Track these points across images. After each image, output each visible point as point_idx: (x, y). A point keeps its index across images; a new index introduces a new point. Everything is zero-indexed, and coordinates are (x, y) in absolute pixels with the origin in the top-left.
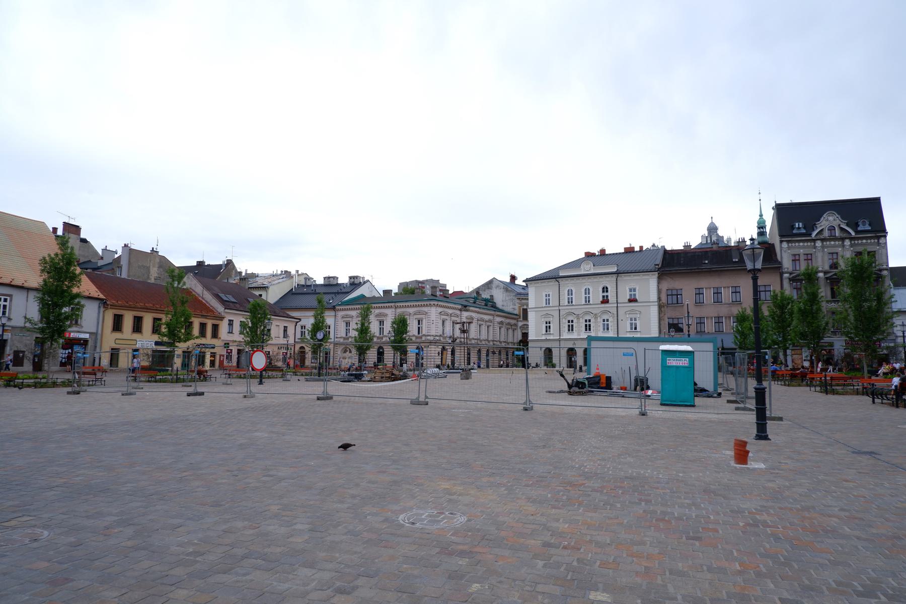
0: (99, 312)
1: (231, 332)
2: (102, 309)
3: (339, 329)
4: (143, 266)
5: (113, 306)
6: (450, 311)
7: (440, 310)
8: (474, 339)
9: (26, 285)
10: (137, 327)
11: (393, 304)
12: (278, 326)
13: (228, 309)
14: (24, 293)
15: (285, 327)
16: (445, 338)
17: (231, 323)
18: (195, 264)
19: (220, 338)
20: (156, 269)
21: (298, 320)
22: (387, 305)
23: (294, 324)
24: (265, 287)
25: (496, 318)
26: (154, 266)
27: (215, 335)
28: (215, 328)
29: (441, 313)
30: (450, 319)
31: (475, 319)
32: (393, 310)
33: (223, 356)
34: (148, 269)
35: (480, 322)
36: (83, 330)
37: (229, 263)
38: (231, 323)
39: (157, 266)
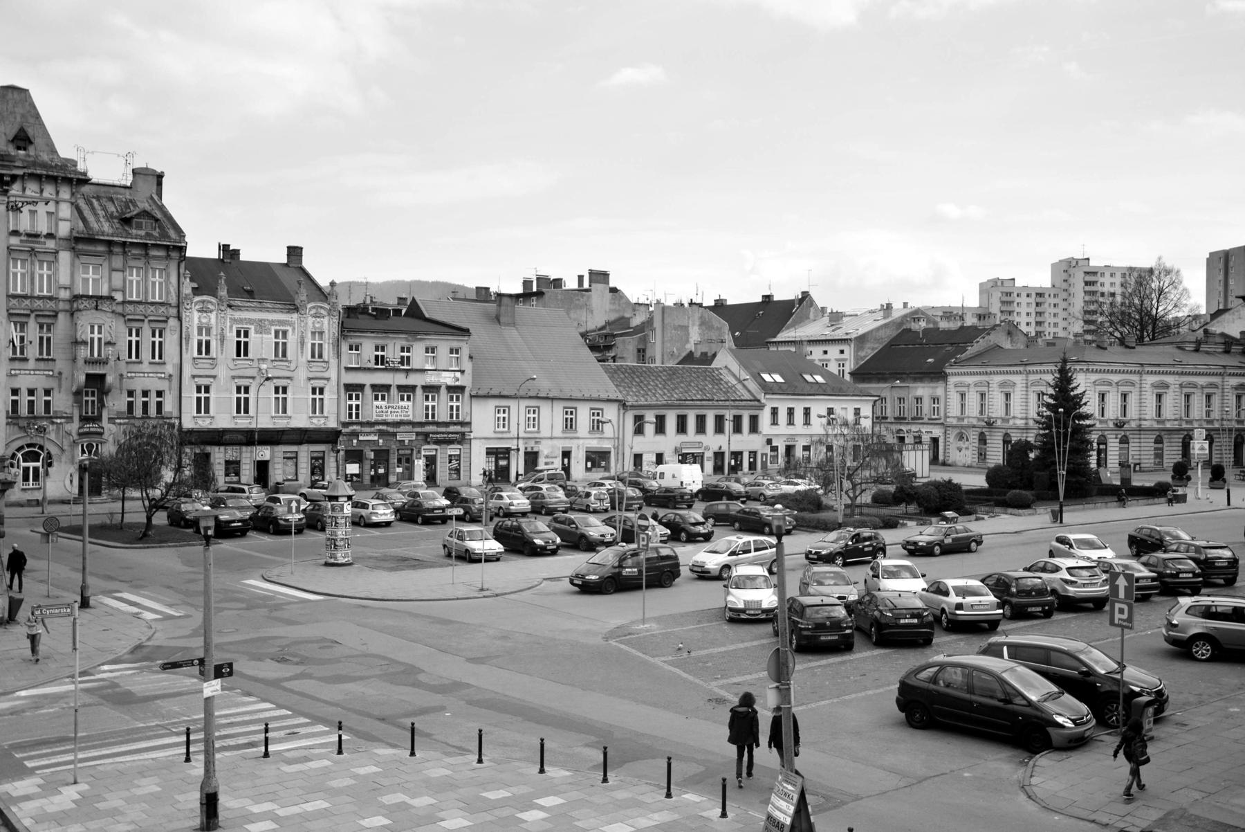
0: (619, 415)
1: (775, 422)
2: (622, 411)
3: (951, 404)
4: (679, 326)
5: (633, 407)
6: (1115, 378)
7: (1094, 377)
8: (1168, 420)
9: (551, 395)
10: (660, 428)
11: (1021, 368)
12: (846, 408)
13: (769, 393)
14: (549, 402)
15: (855, 409)
16: (1106, 422)
17: (775, 412)
18: (760, 300)
19: (761, 433)
20: (696, 328)
21: (877, 398)
22: (1015, 369)
23: (871, 404)
24: (847, 340)
25: (1227, 379)
26: (693, 325)
27: (754, 428)
28: (754, 420)
29: (1094, 382)
30: (1116, 389)
31: (1172, 387)
32: (1023, 376)
33: (766, 455)
34: (685, 328)
35: (1185, 390)
36: (605, 435)
37: (805, 295)
38: (775, 412)
39: (697, 323)
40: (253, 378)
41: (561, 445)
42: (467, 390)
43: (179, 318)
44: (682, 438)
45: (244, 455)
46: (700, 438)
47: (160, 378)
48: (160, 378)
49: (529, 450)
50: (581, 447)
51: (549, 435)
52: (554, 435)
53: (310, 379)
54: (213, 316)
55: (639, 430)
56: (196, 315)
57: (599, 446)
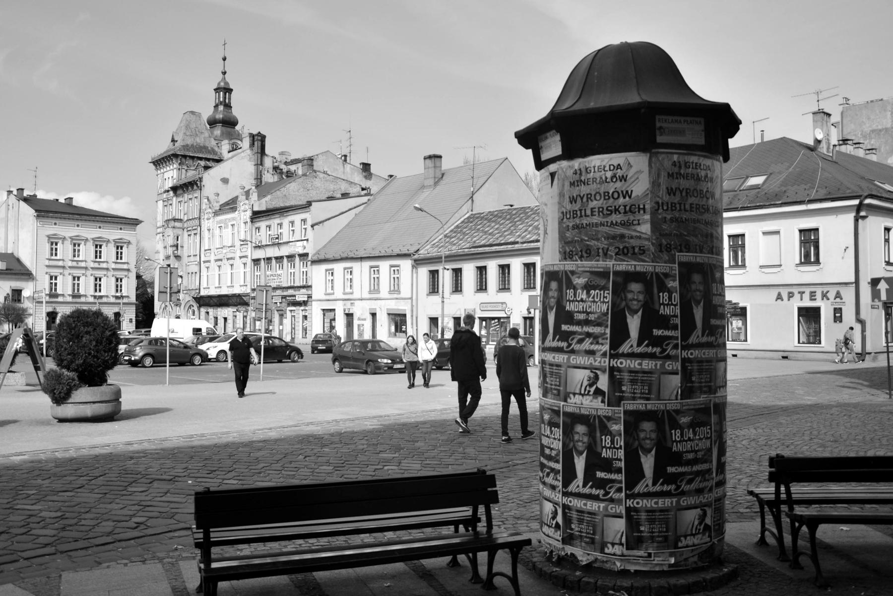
40: (221, 260)
41: (369, 305)
42: (310, 258)
43: (200, 227)
44: (482, 297)
45: (219, 313)
46: (504, 297)
47: (196, 265)
48: (196, 265)
49: (347, 312)
50: (383, 308)
51: (359, 297)
52: (364, 296)
53: (241, 257)
54: (211, 221)
55: (434, 288)
56: (206, 221)
57: (396, 307)
